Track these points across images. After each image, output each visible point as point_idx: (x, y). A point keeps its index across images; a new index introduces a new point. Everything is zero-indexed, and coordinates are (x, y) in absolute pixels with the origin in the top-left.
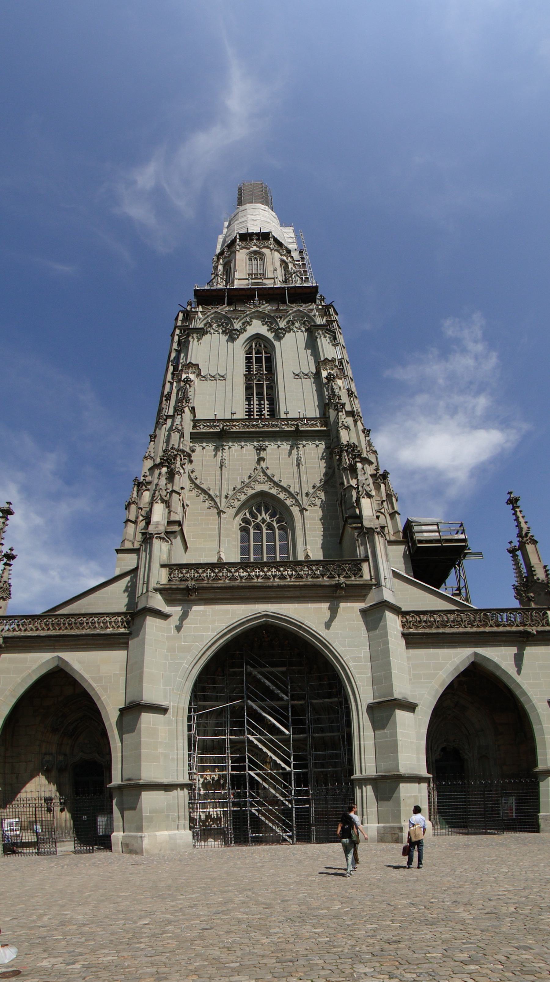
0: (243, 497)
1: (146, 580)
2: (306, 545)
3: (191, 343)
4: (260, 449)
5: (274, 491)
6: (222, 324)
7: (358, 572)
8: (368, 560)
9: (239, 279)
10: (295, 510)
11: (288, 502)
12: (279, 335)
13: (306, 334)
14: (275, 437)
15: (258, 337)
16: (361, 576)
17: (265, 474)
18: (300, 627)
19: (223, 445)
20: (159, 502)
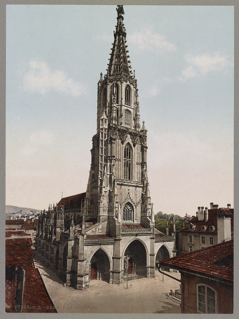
5: (131, 202)
10: (134, 207)
15: (129, 143)
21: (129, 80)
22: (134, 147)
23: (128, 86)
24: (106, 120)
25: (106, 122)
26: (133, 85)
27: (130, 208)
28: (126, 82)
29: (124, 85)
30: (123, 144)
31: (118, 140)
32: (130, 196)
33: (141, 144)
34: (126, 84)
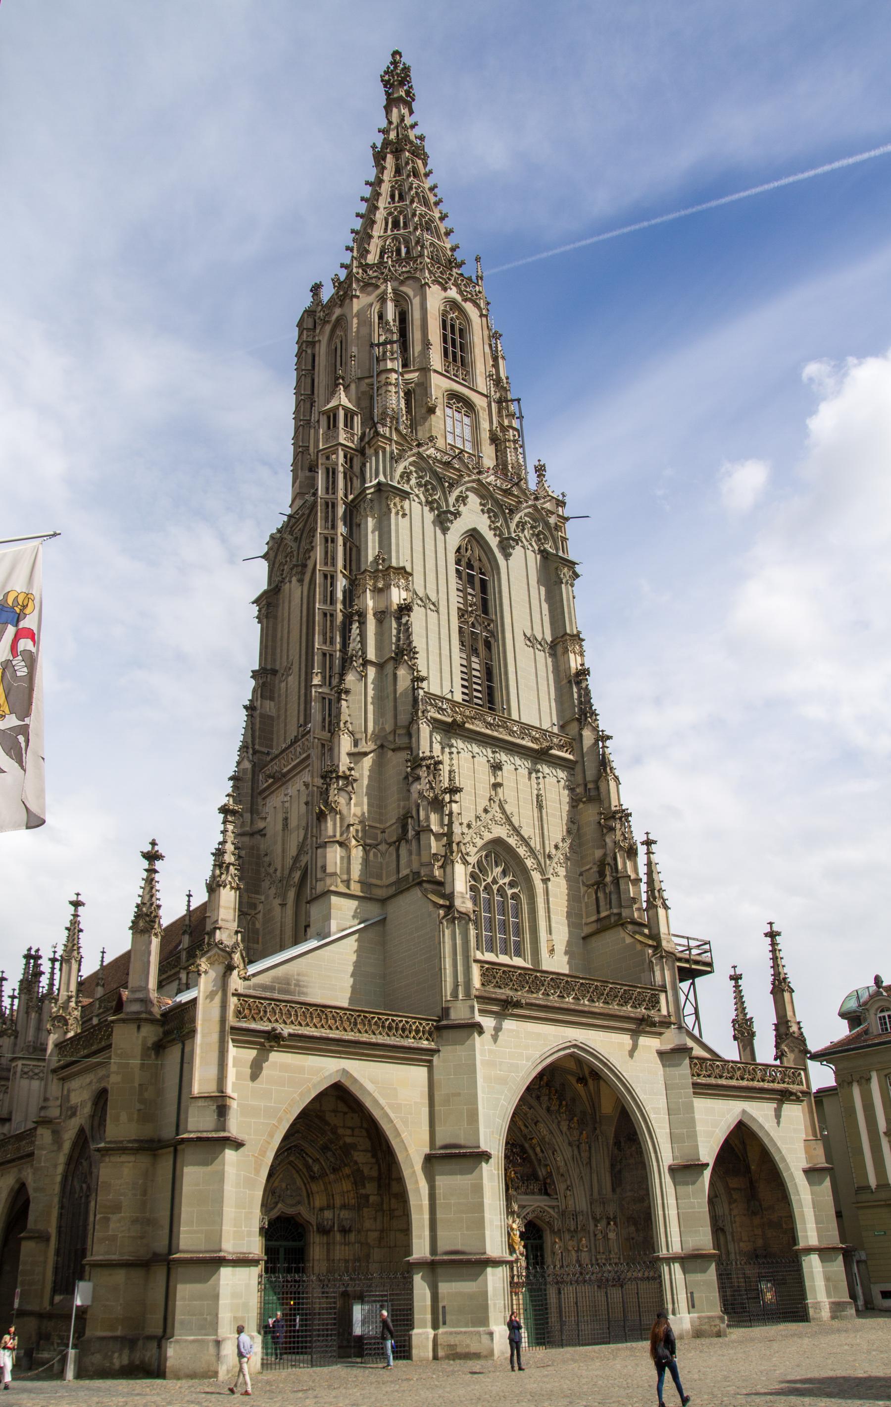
0: (480, 843)
1: (461, 979)
2: (550, 934)
3: (393, 515)
4: (497, 767)
5: (512, 841)
6: (426, 485)
7: (654, 1003)
8: (666, 992)
9: (435, 371)
10: (536, 876)
11: (529, 863)
12: (506, 546)
13: (539, 557)
14: (512, 750)
15: (474, 535)
16: (659, 1010)
17: (504, 812)
18: (605, 1064)
19: (451, 746)
20: (459, 861)
21: (456, 285)
22: (507, 556)
23: (453, 305)
24: (349, 415)
25: (349, 423)
26: (477, 306)
27: (512, 885)
28: (445, 289)
29: (435, 298)
30: (445, 530)
31: (416, 506)
32: (506, 807)
33: (544, 553)
34: (443, 294)
